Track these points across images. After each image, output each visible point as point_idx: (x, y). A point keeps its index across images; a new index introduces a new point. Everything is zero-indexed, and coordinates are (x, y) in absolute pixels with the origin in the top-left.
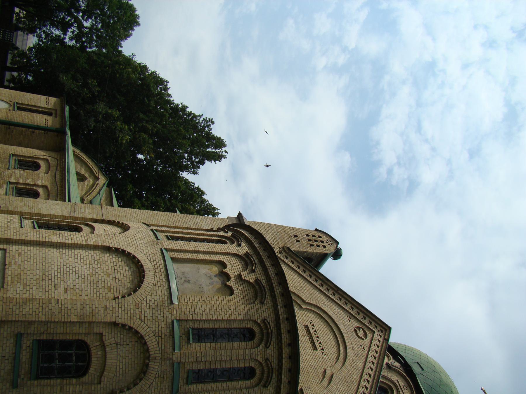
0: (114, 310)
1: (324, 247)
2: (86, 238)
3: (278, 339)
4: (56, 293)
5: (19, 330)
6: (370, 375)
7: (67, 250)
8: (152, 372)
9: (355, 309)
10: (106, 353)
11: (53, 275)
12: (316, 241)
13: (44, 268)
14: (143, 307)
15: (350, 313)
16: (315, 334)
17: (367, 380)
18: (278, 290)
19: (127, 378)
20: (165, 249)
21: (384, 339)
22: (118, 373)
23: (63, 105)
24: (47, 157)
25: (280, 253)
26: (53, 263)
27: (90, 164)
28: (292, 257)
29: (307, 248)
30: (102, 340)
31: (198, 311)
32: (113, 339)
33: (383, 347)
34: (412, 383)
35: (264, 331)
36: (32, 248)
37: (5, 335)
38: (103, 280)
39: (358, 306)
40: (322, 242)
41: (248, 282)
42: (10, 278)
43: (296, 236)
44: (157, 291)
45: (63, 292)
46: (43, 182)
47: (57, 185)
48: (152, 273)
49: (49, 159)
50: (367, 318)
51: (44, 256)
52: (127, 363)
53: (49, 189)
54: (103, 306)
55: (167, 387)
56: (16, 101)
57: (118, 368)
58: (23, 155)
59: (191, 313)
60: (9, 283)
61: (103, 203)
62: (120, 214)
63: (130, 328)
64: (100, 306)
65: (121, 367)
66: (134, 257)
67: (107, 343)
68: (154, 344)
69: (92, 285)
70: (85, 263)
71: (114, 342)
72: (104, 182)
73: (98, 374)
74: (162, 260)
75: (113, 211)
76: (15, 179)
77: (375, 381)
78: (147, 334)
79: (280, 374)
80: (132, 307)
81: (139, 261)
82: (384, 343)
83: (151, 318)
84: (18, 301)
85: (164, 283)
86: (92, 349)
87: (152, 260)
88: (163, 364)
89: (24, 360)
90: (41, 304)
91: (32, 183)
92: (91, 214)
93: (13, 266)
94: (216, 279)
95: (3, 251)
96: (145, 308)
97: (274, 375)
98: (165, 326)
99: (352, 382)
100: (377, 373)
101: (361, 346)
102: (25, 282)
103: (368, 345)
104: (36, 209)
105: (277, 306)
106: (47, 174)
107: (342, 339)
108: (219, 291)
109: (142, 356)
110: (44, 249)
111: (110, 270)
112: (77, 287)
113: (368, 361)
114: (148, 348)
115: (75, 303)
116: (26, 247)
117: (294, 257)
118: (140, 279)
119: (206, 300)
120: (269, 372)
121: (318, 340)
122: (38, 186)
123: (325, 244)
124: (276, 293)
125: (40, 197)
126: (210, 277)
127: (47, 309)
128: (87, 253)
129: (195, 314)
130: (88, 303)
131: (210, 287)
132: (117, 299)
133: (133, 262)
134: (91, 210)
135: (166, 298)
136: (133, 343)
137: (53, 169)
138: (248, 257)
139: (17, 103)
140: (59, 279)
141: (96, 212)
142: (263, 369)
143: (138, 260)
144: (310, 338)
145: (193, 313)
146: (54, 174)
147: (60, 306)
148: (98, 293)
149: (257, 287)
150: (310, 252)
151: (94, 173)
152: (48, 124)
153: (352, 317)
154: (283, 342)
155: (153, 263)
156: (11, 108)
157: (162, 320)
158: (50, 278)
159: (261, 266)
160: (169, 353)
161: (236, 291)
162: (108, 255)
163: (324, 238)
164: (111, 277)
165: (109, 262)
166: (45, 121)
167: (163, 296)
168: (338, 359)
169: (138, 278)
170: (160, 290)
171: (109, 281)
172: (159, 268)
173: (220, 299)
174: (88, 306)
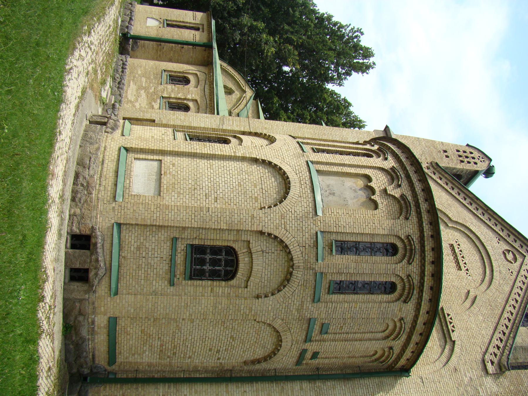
0: (261, 219)
1: (476, 163)
2: (234, 150)
3: (421, 256)
4: (207, 202)
5: (175, 235)
6: (517, 301)
7: (217, 161)
8: (296, 280)
9: (505, 231)
10: (252, 260)
11: (204, 185)
12: (467, 157)
13: (195, 178)
14: (288, 218)
15: (499, 235)
16: (460, 254)
17: (513, 305)
18: (424, 206)
19: (271, 285)
20: (310, 161)
22: (263, 279)
25: (428, 168)
26: (203, 174)
28: (440, 173)
29: (456, 164)
30: (249, 247)
31: (342, 223)
32: (259, 247)
35: (408, 247)
36: (184, 159)
37: (163, 239)
38: (250, 190)
39: (508, 228)
40: (473, 158)
41: (394, 197)
42: (165, 187)
43: (445, 151)
44: (303, 202)
45: (213, 201)
46: (193, 96)
48: (298, 185)
49: (198, 73)
50: (518, 241)
51: (195, 166)
52: (272, 271)
53: (199, 102)
54: (250, 215)
55: (309, 295)
56: (165, 18)
57: (263, 274)
59: (335, 225)
60: (165, 192)
61: (250, 115)
62: (266, 126)
63: (276, 237)
64: (247, 215)
65: (266, 273)
66: (280, 169)
67: (253, 250)
68: (297, 253)
69: (240, 195)
70: (234, 174)
71: (261, 250)
73: (245, 279)
74: (308, 173)
76: (167, 94)
77: (522, 307)
78: (292, 244)
79: (421, 291)
80: (277, 217)
81: (285, 173)
83: (296, 228)
84: (173, 209)
85: (309, 195)
86: (239, 255)
87: (297, 172)
88: (306, 274)
89: (179, 262)
90: (193, 212)
93: (168, 176)
94: (361, 193)
95: (159, 162)
96: (291, 218)
97: (415, 292)
98: (309, 237)
99: (496, 306)
101: (509, 270)
102: (179, 191)
103: (517, 269)
105: (422, 222)
106: (197, 88)
108: (363, 204)
109: (286, 264)
110: (195, 160)
111: (257, 181)
112: (226, 196)
113: (516, 286)
114: (292, 257)
115: (225, 211)
116: (179, 158)
117: (443, 173)
118: (286, 190)
119: (350, 213)
120: (410, 289)
121: (463, 261)
122: (188, 100)
123: (476, 161)
124: (422, 209)
126: (355, 191)
127: (199, 217)
128: (235, 164)
129: (339, 226)
130: (236, 212)
131: (355, 201)
132: (263, 209)
133: (279, 174)
135: (311, 209)
136: (278, 252)
137: (202, 83)
138: (394, 172)
139: (166, 20)
140: (210, 188)
142: (404, 284)
143: (284, 171)
144: (454, 258)
145: (337, 226)
146: (203, 88)
147: (211, 214)
148: (246, 203)
149: (402, 202)
150: (460, 169)
153: (501, 239)
154: (426, 260)
155: (298, 175)
156: (161, 25)
157: (307, 231)
158: (201, 187)
159: (408, 181)
160: (312, 263)
161: (380, 206)
162: (255, 166)
163: (476, 154)
164: (258, 187)
165: (256, 174)
167: (308, 207)
168: (483, 281)
169: (284, 189)
170: (305, 201)
171: (256, 191)
172: (304, 180)
173: (364, 213)
174: (236, 215)
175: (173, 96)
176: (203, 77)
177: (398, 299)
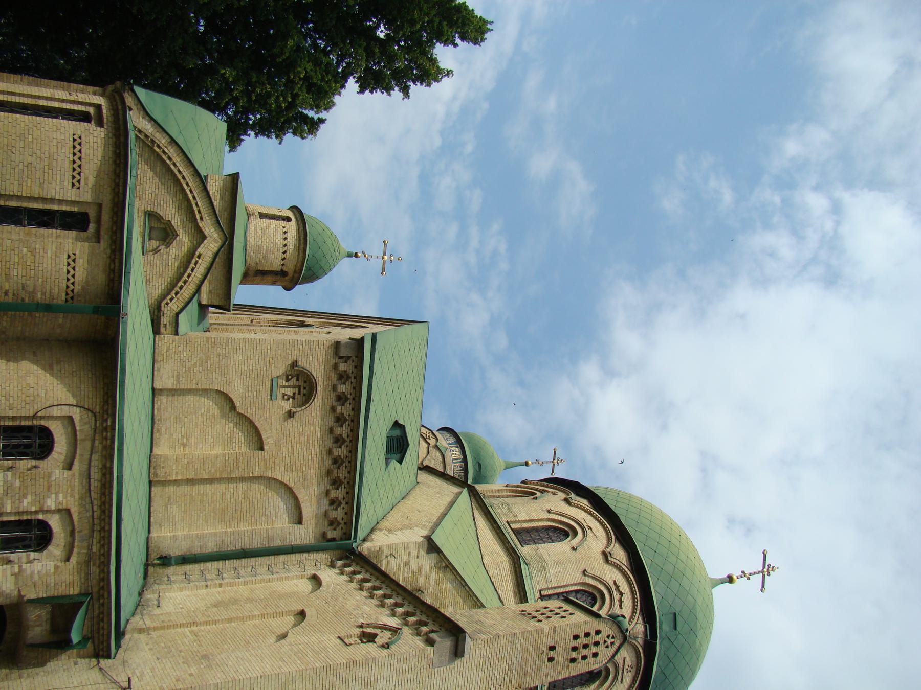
12: (586, 646)
23: (121, 191)
24: (71, 408)
27: (187, 184)
34: (645, 662)
40: (596, 644)
46: (61, 497)
47: (92, 503)
49: (76, 414)
53: (75, 517)
58: (11, 414)
72: (216, 249)
91: (33, 509)
106: (70, 468)
125: (54, 541)
137: (83, 449)
151: (194, 216)
152: (73, 276)
166: (69, 264)
175: (8, 511)
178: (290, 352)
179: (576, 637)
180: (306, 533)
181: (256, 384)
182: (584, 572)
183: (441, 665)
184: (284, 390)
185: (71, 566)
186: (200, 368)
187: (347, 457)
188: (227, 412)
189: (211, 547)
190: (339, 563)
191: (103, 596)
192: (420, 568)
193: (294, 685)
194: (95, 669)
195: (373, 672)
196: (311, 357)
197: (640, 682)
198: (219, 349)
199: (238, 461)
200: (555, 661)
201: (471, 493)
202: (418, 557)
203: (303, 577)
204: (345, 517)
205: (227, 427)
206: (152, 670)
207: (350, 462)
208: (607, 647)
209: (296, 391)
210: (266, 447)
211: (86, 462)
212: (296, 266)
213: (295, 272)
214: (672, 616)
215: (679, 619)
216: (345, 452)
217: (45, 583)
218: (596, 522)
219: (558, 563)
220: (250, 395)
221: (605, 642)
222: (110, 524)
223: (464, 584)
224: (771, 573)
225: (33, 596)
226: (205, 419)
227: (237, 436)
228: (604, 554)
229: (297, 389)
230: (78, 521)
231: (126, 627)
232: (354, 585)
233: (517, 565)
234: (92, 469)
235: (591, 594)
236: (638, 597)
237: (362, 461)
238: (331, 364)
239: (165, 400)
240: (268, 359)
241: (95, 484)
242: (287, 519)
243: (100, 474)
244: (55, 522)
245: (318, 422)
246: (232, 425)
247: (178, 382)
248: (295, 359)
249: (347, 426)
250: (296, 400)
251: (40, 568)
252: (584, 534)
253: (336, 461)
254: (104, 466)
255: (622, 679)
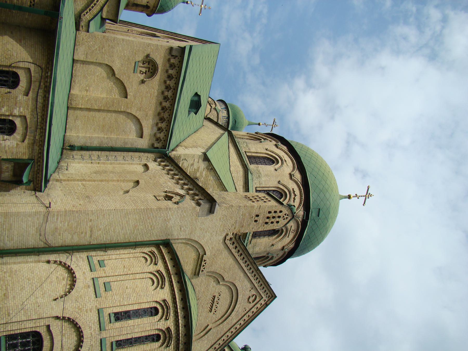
12: (274, 217)
15: (254, 285)
21: (266, 303)
24: (30, 64)
33: (260, 310)
34: (301, 230)
39: (264, 281)
46: (22, 109)
47: (37, 114)
49: (32, 67)
53: (28, 120)
75: (86, 216)
82: (263, 307)
91: (7, 114)
92: (63, 223)
100: (242, 328)
103: (251, 307)
104: (7, 225)
106: (27, 95)
107: (235, 304)
125: (17, 131)
134: (63, 217)
137: (35, 86)
141: (69, 220)
168: (222, 317)
176: (37, 75)
177: (161, 318)
178: (146, 49)
179: (270, 212)
180: (144, 143)
181: (127, 64)
182: (279, 182)
183: (202, 216)
184: (141, 69)
185: (25, 145)
186: (99, 52)
187: (169, 107)
188: (111, 77)
189: (96, 144)
190: (159, 160)
191: (40, 161)
192: (199, 168)
193: (130, 216)
194: (33, 196)
195: (169, 214)
196: (157, 53)
197: (297, 238)
198: (109, 43)
199: (113, 102)
200: (258, 222)
201: (229, 135)
202: (198, 162)
203: (140, 164)
204: (164, 137)
205: (110, 84)
206: (62, 200)
207: (170, 110)
208: (284, 219)
209: (147, 70)
210: (128, 97)
211: (36, 93)
212: (155, 3)
213: (154, 7)
214: (318, 210)
215: (321, 212)
216: (169, 105)
217: (11, 152)
218: (289, 158)
219: (267, 175)
220: (123, 69)
221: (283, 217)
222: (46, 126)
223: (219, 179)
224: (370, 197)
225: (5, 157)
226: (99, 79)
227: (115, 89)
228: (290, 174)
229: (148, 69)
230: (30, 123)
231: (50, 178)
232: (165, 172)
233: (246, 173)
234: (39, 97)
235: (280, 193)
236: (303, 198)
237: (177, 111)
238: (167, 59)
239: (79, 66)
240: (135, 51)
241: (39, 105)
242: (135, 134)
243: (42, 100)
244: (18, 122)
245: (157, 87)
246: (113, 83)
247: (87, 57)
248: (149, 53)
249: (171, 91)
250: (147, 75)
251: (9, 144)
252: (282, 163)
253: (163, 109)
254: (45, 96)
255: (288, 236)
